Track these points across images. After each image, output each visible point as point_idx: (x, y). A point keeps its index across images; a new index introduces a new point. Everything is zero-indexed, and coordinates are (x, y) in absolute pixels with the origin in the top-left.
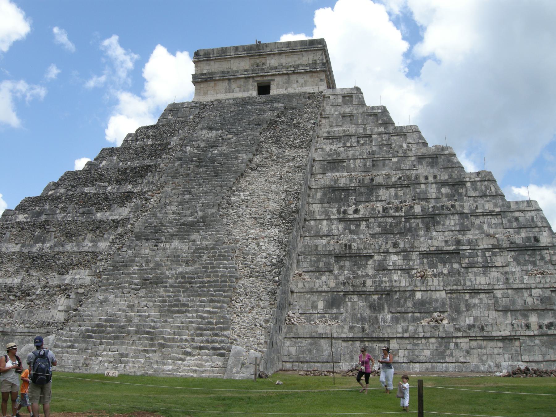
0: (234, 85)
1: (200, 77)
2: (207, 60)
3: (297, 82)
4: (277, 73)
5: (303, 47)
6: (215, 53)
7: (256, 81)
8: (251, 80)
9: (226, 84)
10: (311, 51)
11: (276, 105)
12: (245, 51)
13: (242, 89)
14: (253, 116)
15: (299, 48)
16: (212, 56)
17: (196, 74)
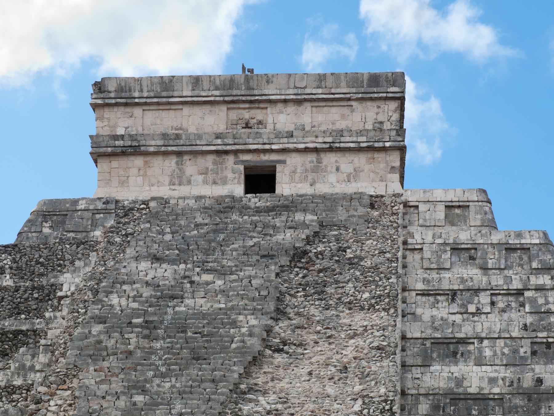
0: (191, 167)
1: (111, 143)
2: (126, 105)
3: (338, 169)
4: (291, 146)
5: (354, 90)
6: (145, 89)
7: (243, 162)
8: (231, 159)
9: (171, 163)
10: (371, 99)
11: (299, 217)
12: (217, 89)
13: (211, 177)
14: (252, 237)
15: (345, 91)
16: (136, 94)
17: (97, 136)
